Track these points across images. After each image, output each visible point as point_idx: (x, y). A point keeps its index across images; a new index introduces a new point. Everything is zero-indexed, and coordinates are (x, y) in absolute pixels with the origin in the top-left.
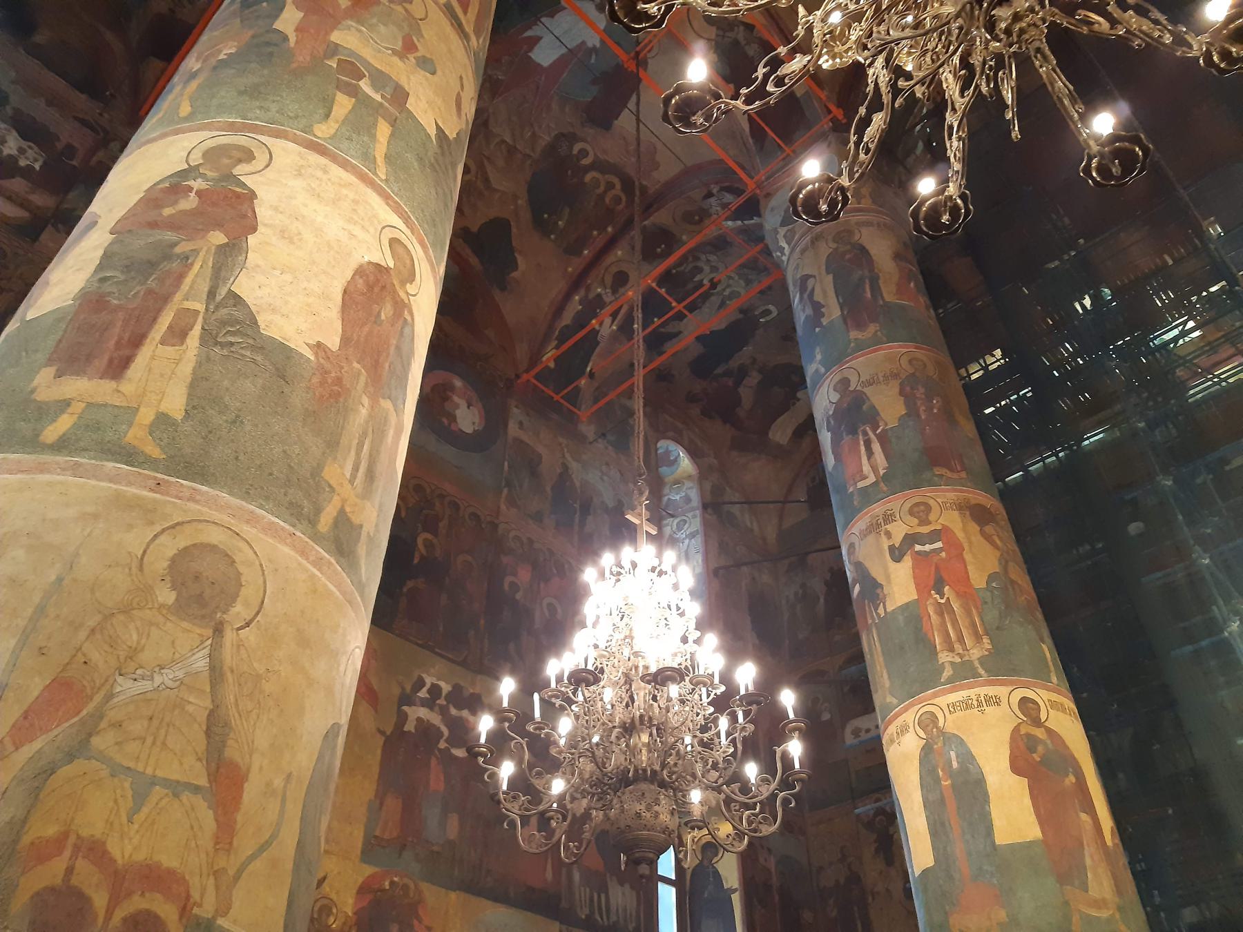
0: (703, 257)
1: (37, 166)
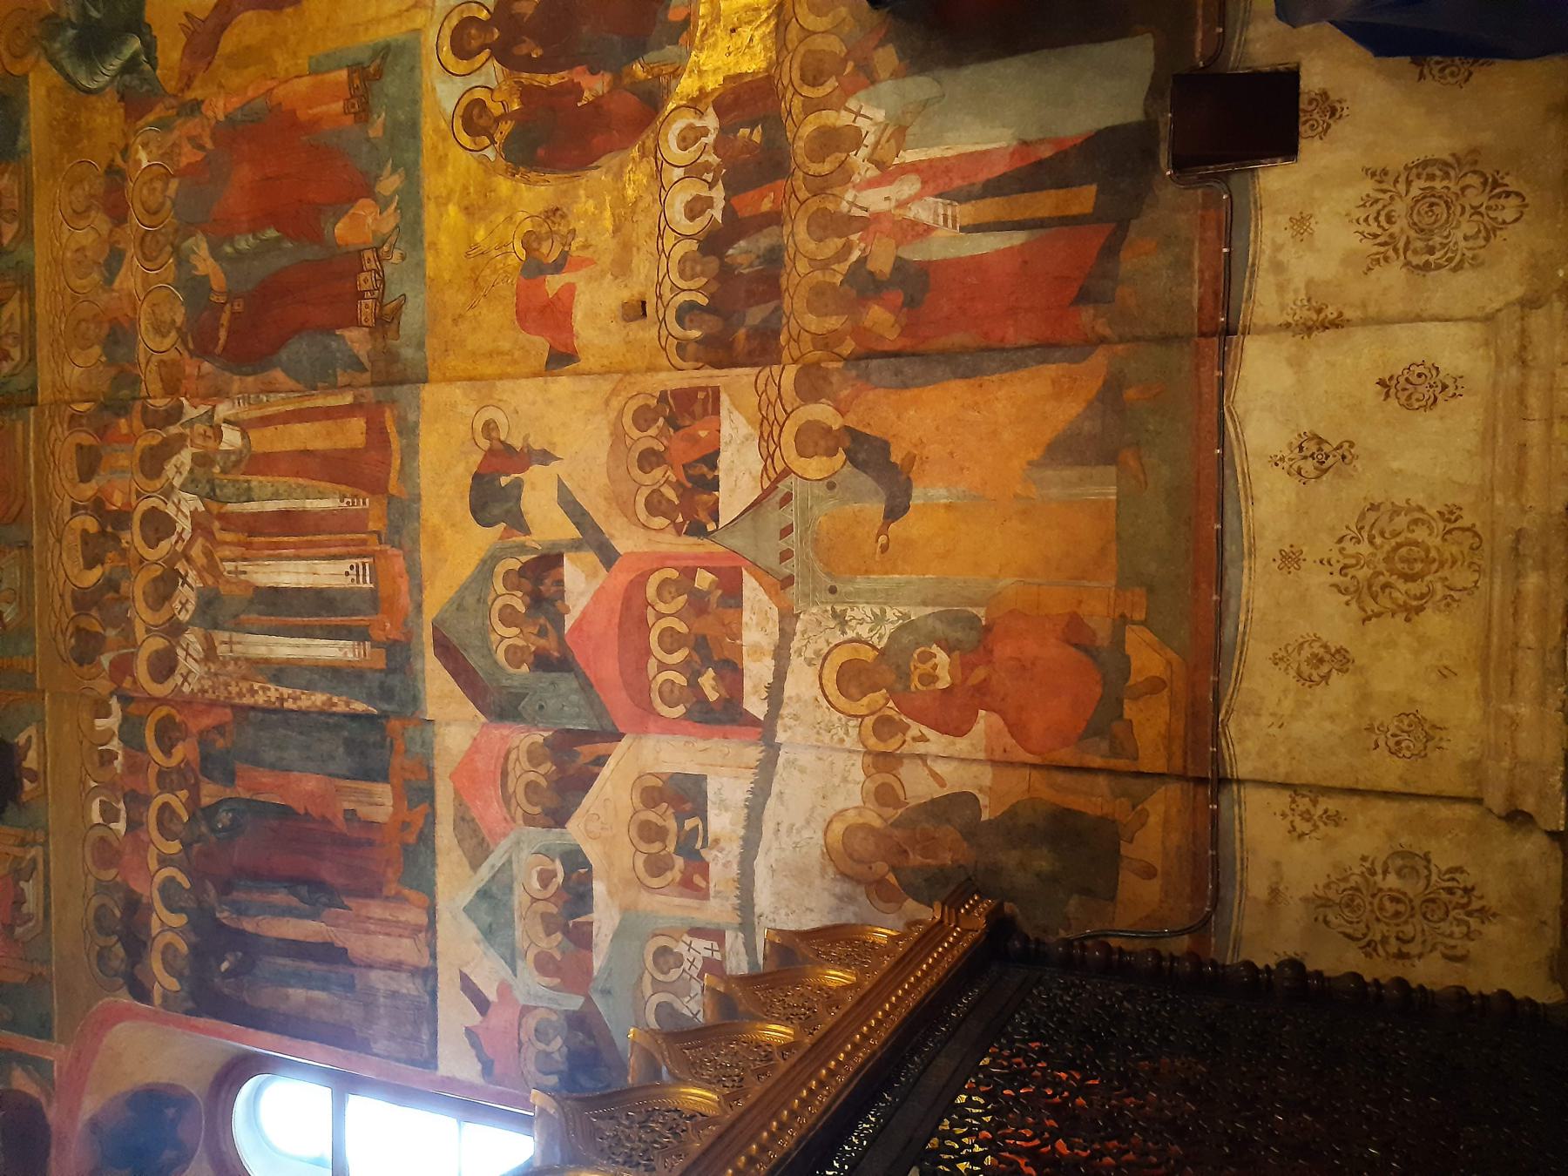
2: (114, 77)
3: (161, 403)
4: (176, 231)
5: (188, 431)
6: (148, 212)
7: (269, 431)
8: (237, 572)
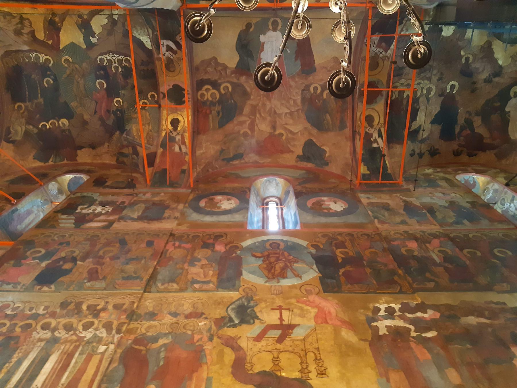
0: (398, 84)
1: (110, 211)
2: (229, 315)
3: (124, 328)
4: (175, 333)
5: (111, 336)
6: (185, 325)
7: (97, 361)
8: (60, 349)
